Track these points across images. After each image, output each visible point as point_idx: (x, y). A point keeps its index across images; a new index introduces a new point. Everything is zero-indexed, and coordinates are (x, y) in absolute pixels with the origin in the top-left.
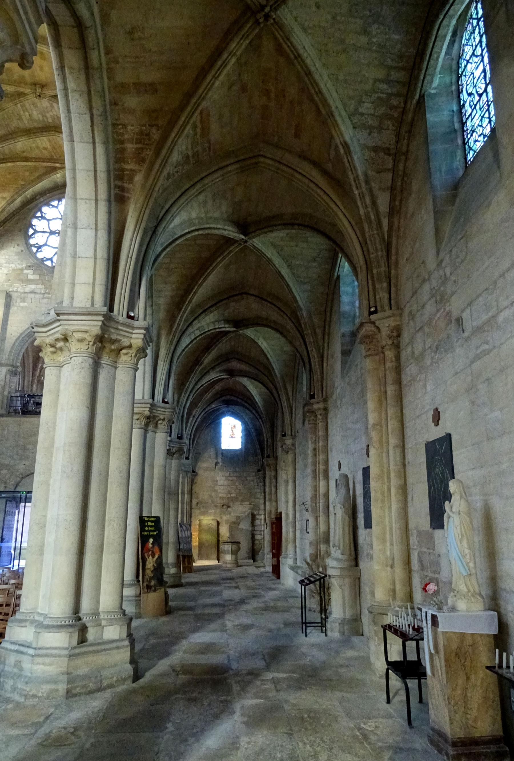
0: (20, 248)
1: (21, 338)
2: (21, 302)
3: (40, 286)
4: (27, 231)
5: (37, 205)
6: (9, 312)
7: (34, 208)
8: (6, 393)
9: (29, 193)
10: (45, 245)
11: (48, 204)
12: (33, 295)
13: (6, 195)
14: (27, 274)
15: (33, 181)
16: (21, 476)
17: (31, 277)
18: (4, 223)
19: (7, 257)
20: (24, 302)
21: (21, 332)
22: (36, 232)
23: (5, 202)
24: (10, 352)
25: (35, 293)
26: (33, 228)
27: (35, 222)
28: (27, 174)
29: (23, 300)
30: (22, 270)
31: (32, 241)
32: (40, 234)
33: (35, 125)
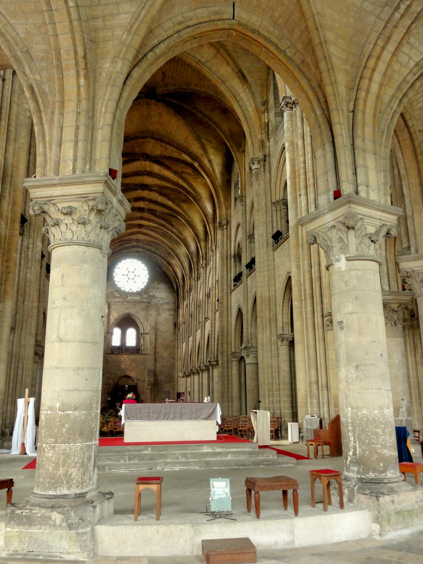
17: (117, 295)
29: (115, 305)
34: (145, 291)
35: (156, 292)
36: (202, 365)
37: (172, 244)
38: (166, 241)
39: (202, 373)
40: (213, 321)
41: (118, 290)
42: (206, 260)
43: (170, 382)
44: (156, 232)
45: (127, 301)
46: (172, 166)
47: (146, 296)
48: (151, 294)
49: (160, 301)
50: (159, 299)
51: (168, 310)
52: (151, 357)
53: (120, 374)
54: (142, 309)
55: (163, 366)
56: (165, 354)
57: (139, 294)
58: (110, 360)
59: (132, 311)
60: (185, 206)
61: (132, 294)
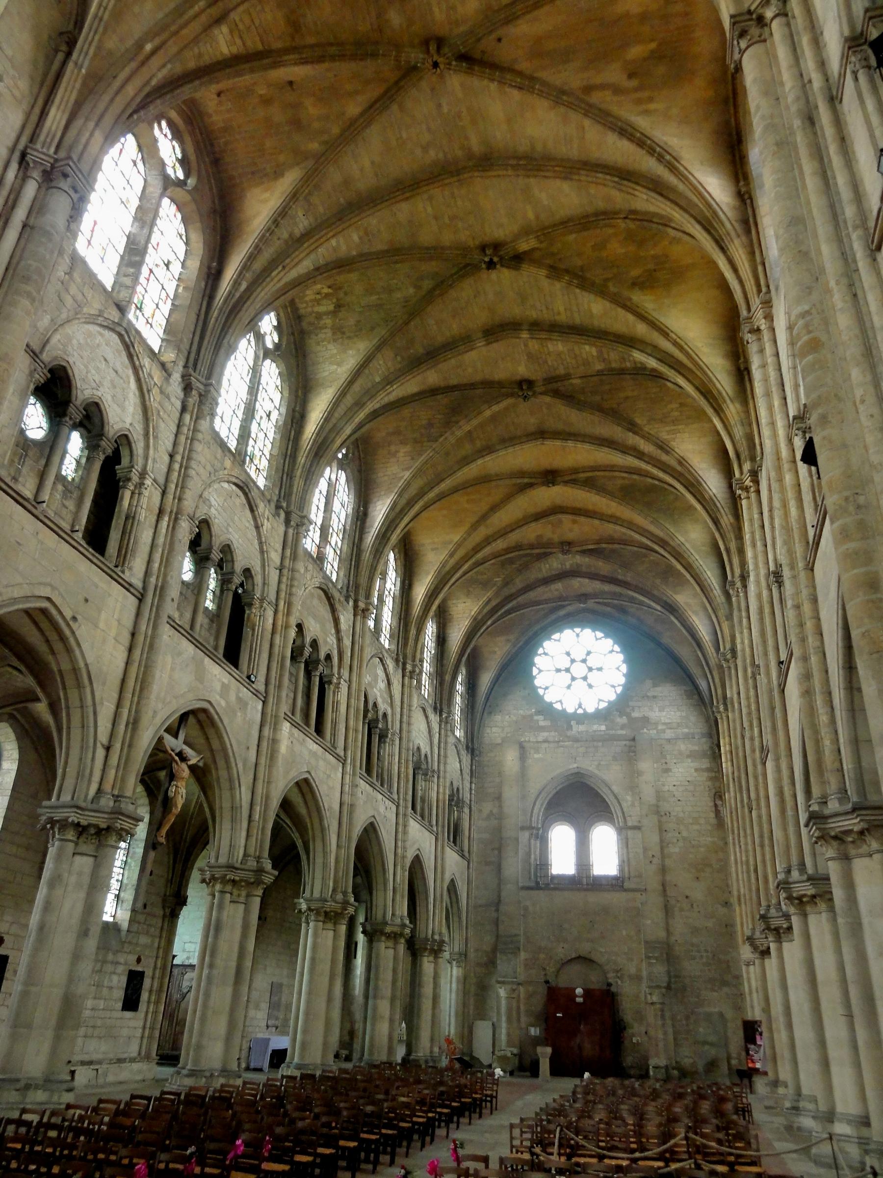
3: (553, 734)
12: (546, 745)
17: (542, 723)
22: (540, 671)
29: (537, 751)
30: (531, 716)
33: (554, 573)
34: (621, 705)
35: (651, 709)
36: (795, 875)
37: (655, 522)
38: (640, 520)
39: (805, 915)
40: (807, 608)
41: (547, 710)
42: (753, 459)
43: (725, 983)
44: (602, 490)
46: (541, 74)
47: (624, 720)
48: (635, 714)
49: (664, 731)
50: (660, 727)
51: (692, 755)
52: (654, 901)
53: (562, 951)
54: (615, 759)
55: (695, 931)
56: (698, 893)
57: (600, 716)
58: (531, 909)
59: (588, 765)
60: (646, 301)
61: (583, 718)
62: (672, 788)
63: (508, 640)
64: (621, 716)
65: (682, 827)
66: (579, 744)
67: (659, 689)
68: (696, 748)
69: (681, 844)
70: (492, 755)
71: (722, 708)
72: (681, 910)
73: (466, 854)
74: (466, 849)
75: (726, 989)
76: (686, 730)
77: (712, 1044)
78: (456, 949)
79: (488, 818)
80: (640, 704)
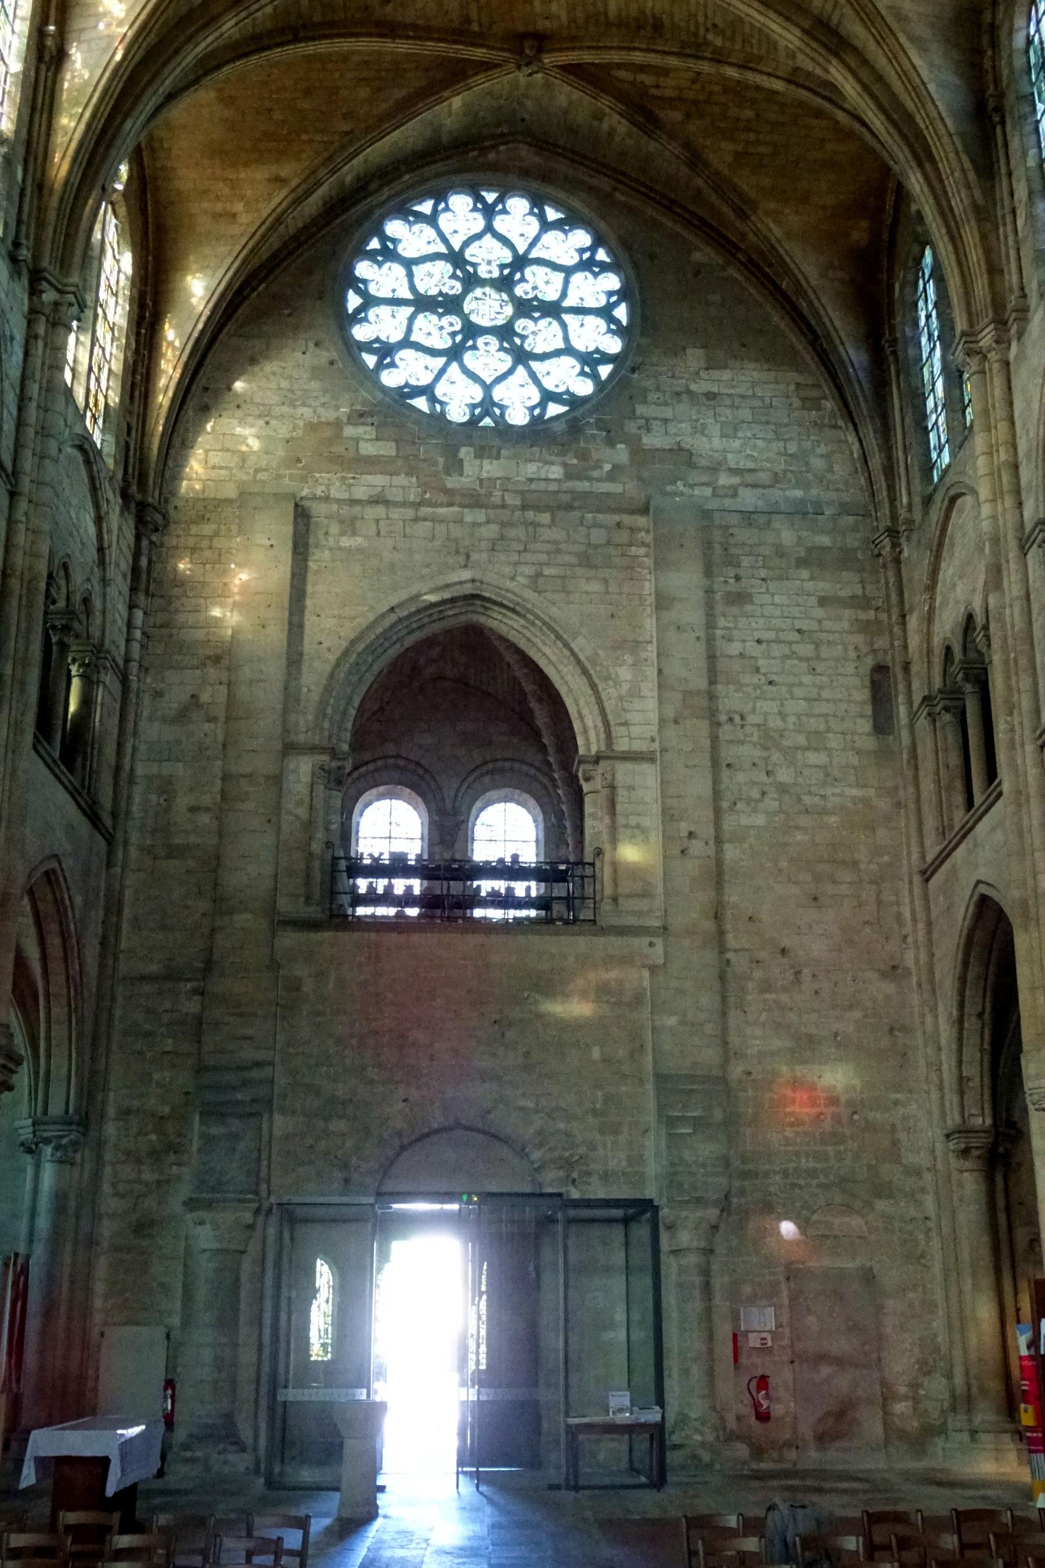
0: (324, 356)
1: (353, 658)
2: (343, 533)
3: (401, 480)
4: (344, 300)
5: (368, 213)
6: (306, 567)
7: (359, 222)
8: (317, 847)
9: (351, 170)
10: (406, 343)
11: (404, 212)
12: (380, 511)
13: (291, 170)
14: (357, 440)
15: (381, 120)
16: (396, 1142)
17: (368, 449)
18: (270, 272)
19: (284, 384)
20: (354, 534)
21: (353, 635)
22: (370, 301)
23: (284, 192)
24: (323, 702)
25: (387, 503)
26: (358, 292)
27: (363, 269)
28: (364, 93)
29: (350, 526)
30: (337, 425)
31: (360, 333)
32: (384, 311)
35: (701, 430)
45: (451, 496)
48: (652, 441)
50: (724, 480)
54: (586, 560)
58: (308, 987)
62: (751, 648)
63: (279, 181)
64: (611, 443)
65: (776, 756)
66: (480, 516)
67: (726, 375)
68: (825, 540)
69: (771, 803)
70: (208, 529)
71: (986, 339)
72: (766, 987)
73: (108, 822)
74: (106, 800)
75: (881, 1205)
76: (798, 493)
77: (839, 1362)
78: (56, 1108)
79: (183, 715)
80: (668, 412)
